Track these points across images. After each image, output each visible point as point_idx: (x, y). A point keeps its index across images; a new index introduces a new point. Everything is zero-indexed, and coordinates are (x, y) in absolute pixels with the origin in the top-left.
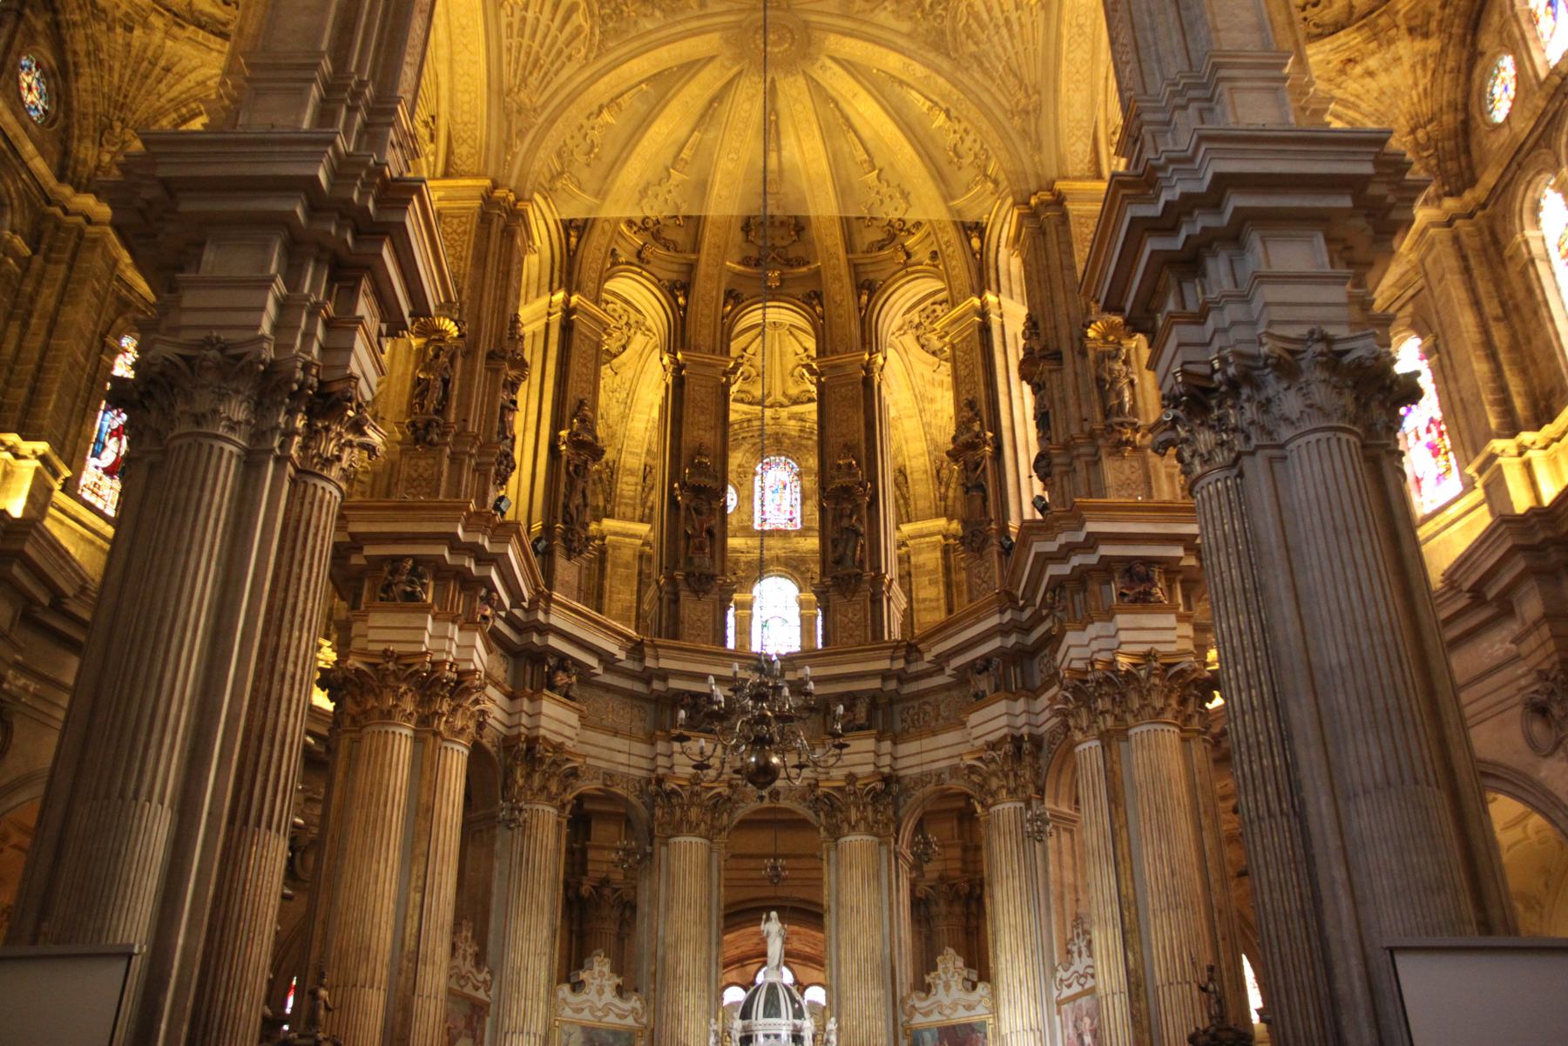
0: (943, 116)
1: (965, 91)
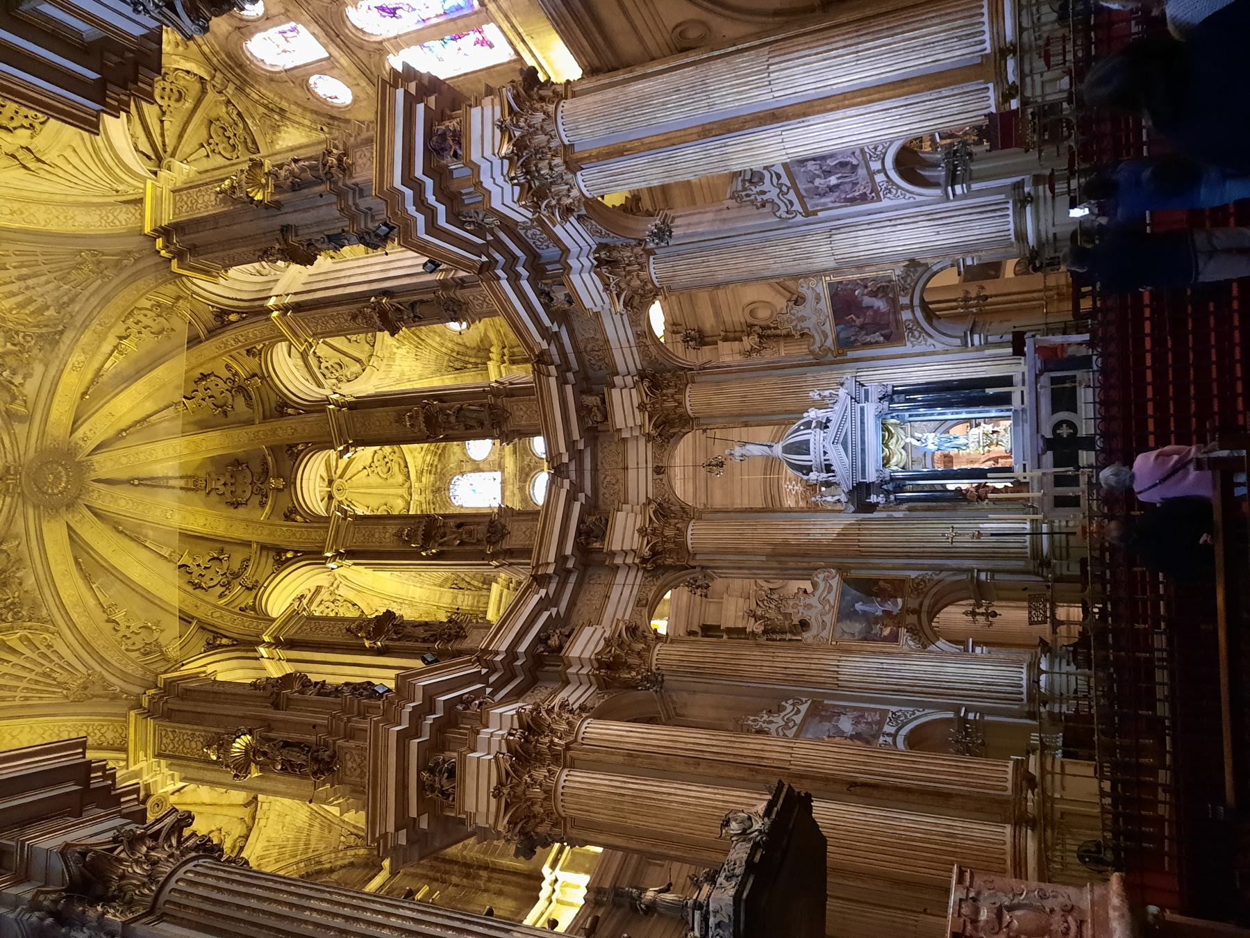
0: (124, 342)
1: (90, 318)
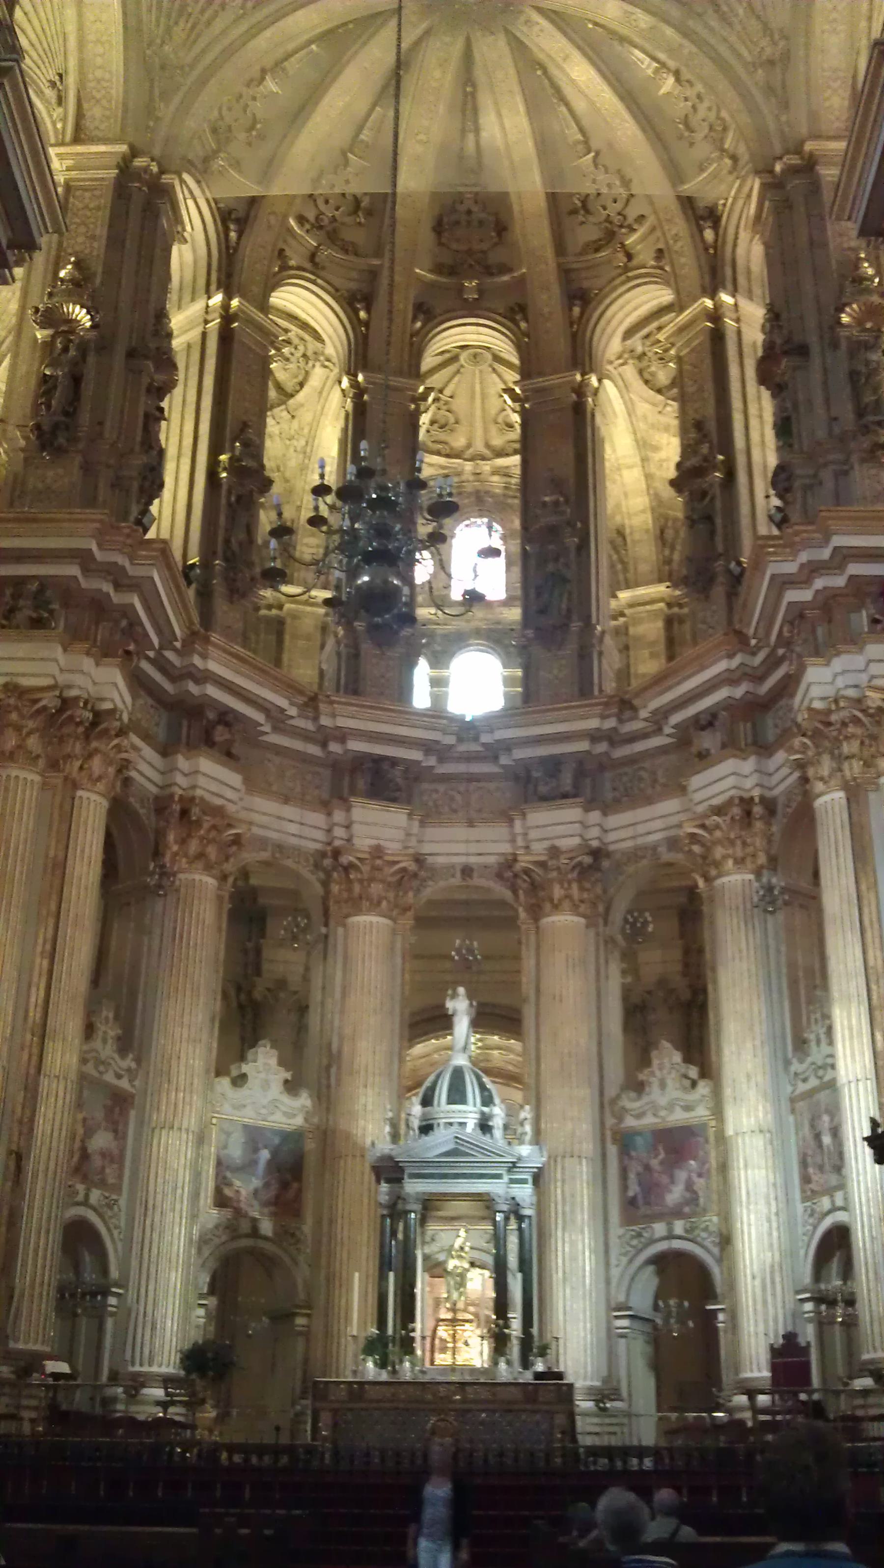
0: (671, 80)
